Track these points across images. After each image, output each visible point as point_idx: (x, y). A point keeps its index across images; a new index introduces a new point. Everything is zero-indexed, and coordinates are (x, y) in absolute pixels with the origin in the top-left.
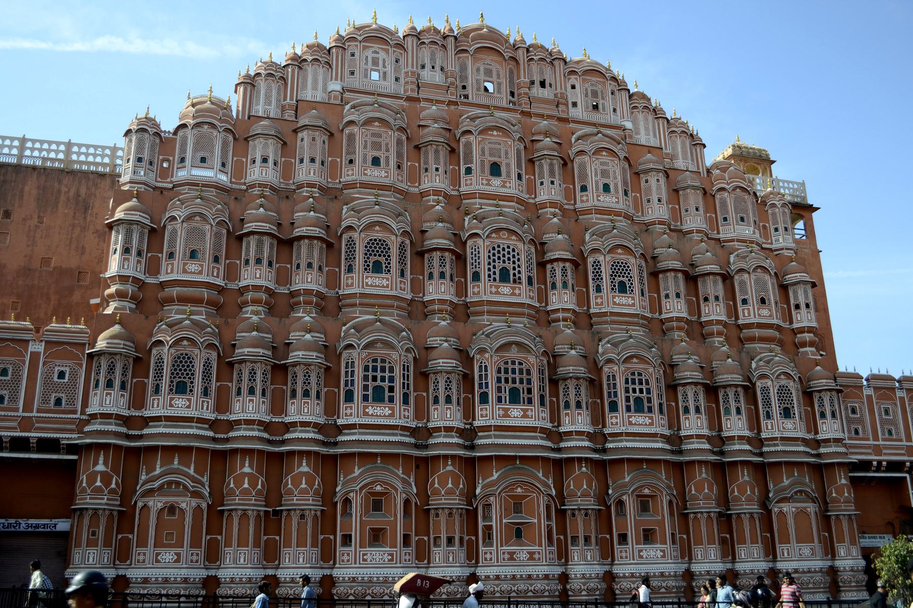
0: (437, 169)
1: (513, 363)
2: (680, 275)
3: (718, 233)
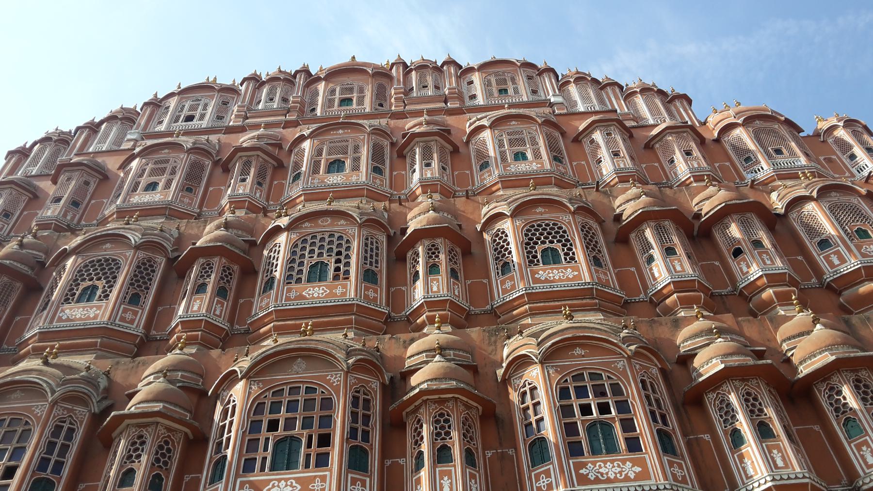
1: (294, 390)
2: (667, 223)
3: (742, 178)
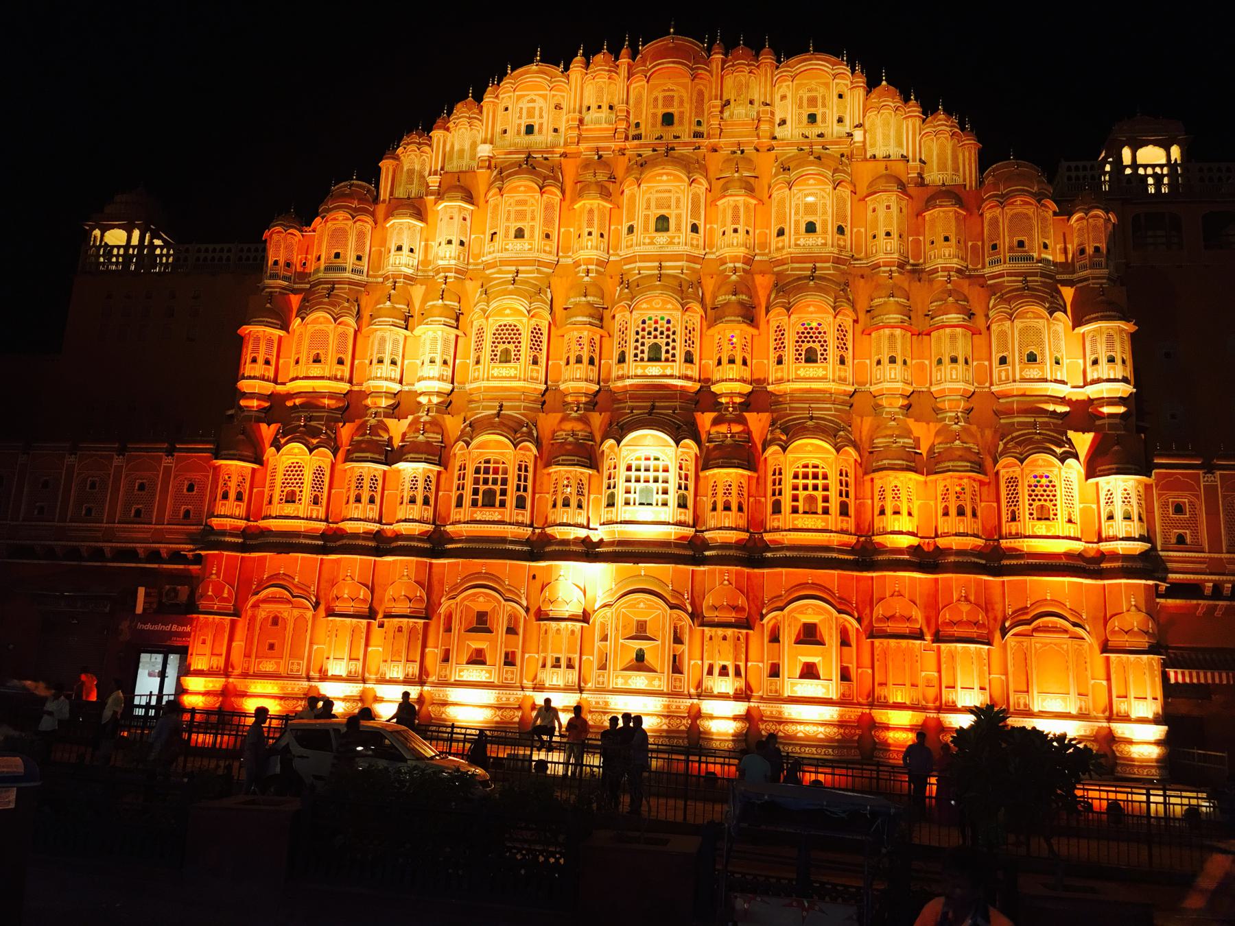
0: (590, 234)
